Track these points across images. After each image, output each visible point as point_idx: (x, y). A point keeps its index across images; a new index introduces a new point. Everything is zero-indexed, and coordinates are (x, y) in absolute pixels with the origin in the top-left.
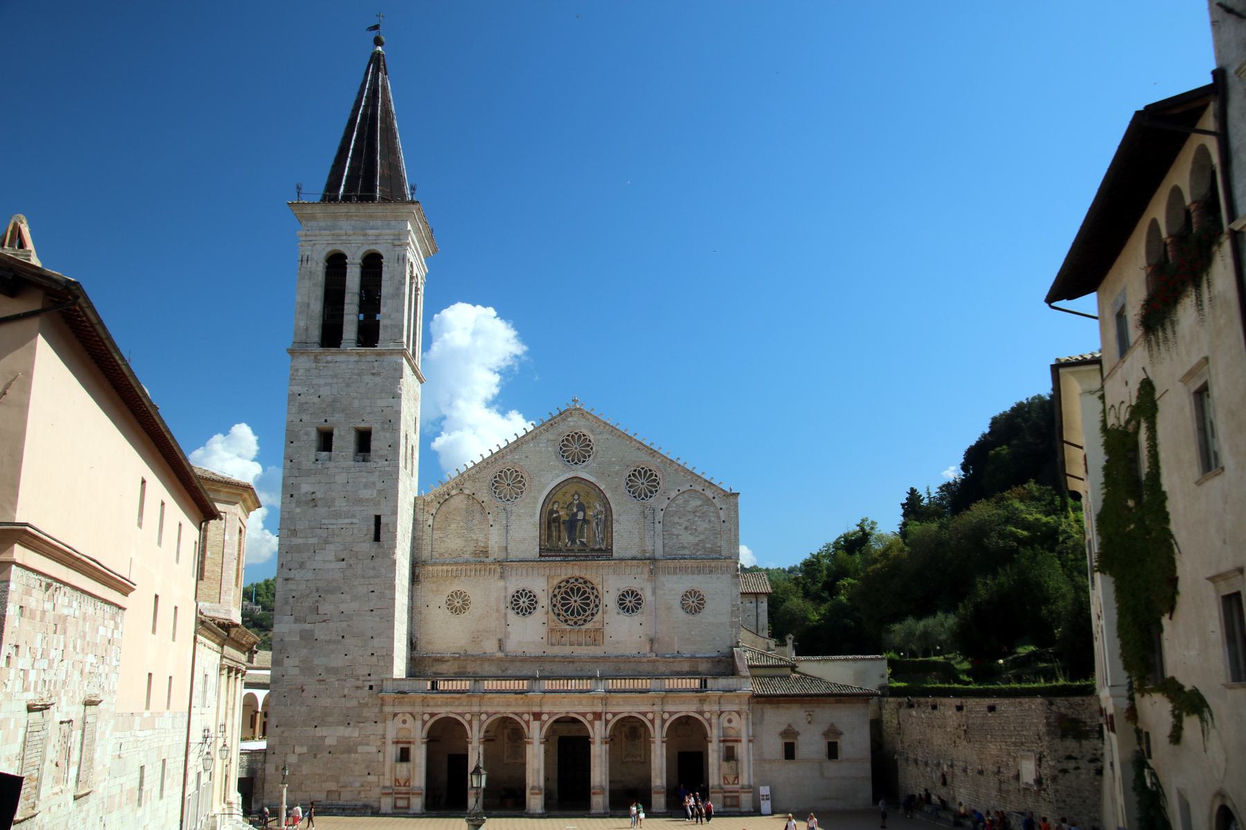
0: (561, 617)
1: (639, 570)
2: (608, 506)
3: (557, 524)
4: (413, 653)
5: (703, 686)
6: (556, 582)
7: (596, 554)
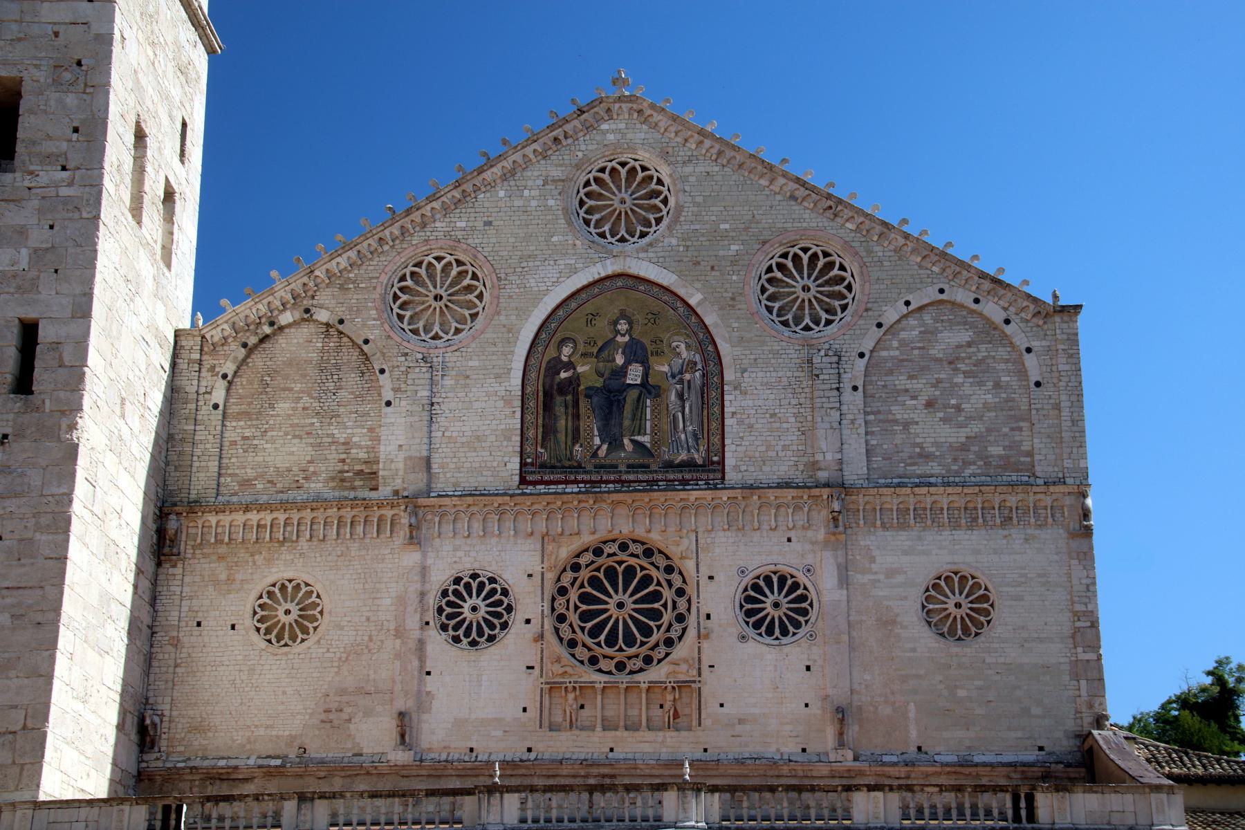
0: (579, 650)
1: (801, 519)
2: (711, 348)
3: (569, 398)
4: (145, 757)
5: (1023, 813)
6: (564, 552)
7: (680, 476)
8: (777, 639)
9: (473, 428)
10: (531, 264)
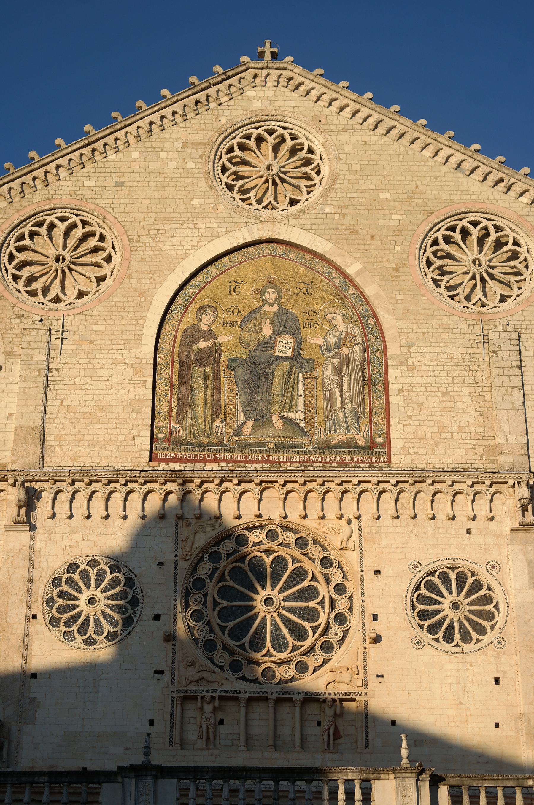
2: (371, 321)
3: (209, 369)
7: (338, 458)
8: (457, 646)
9: (96, 398)
10: (167, 227)
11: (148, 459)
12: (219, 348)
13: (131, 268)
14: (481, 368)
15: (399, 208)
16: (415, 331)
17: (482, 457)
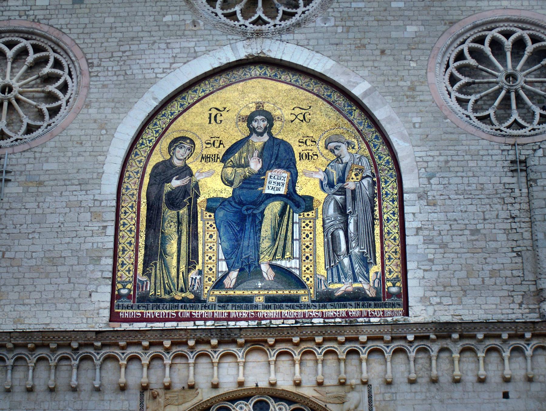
2: (383, 149)
3: (184, 211)
9: (46, 248)
10: (134, 48)
11: (107, 319)
12: (197, 186)
13: (91, 96)
14: (518, 200)
15: (415, 18)
16: (437, 159)
17: (520, 305)
